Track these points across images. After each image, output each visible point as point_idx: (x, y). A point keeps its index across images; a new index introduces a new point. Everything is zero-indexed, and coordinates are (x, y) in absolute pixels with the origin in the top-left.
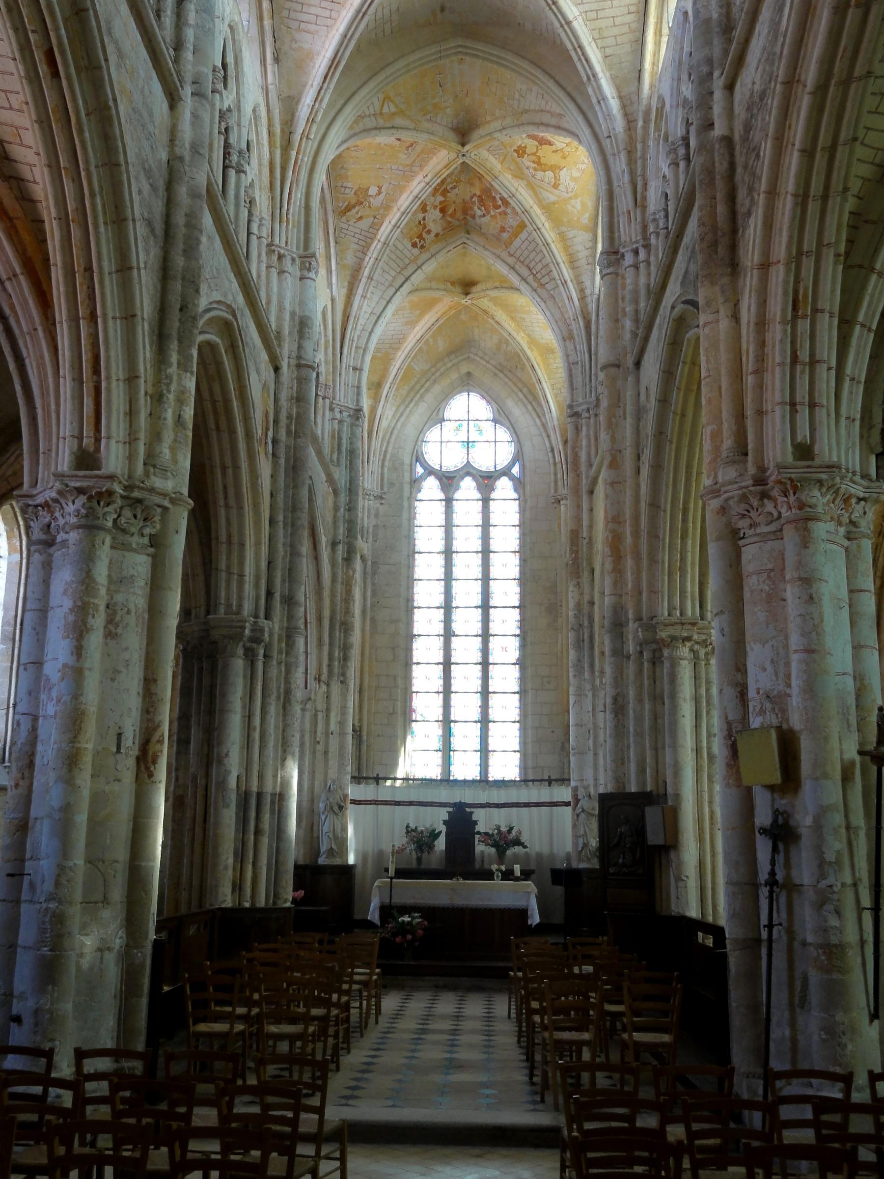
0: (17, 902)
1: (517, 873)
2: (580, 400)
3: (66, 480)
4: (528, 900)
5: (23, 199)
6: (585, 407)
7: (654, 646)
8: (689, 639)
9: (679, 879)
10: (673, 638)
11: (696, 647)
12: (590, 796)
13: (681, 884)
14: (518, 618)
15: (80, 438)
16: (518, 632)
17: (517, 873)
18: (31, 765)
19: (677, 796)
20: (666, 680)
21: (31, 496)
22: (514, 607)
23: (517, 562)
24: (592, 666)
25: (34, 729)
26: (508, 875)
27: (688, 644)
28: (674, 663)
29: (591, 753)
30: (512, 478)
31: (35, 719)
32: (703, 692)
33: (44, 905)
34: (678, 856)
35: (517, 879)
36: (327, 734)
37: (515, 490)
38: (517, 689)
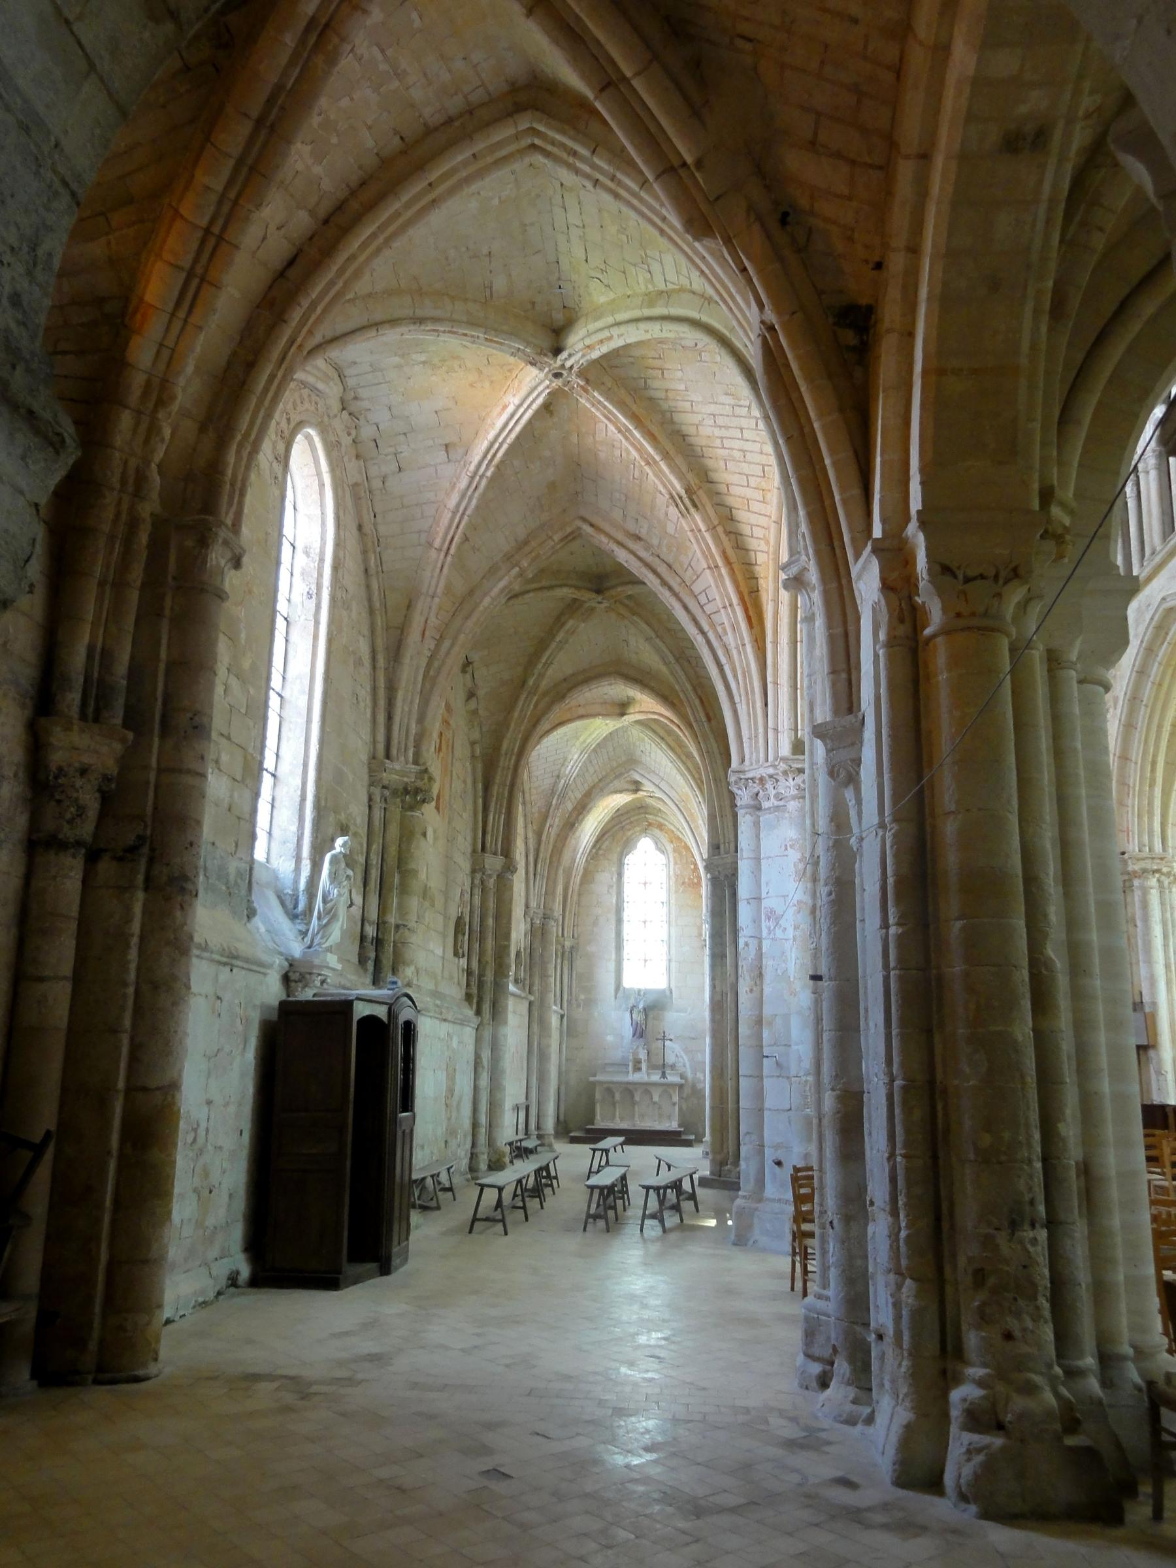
0: (761, 1078)
3: (790, 763)
5: (738, 547)
7: (1126, 877)
8: (1158, 871)
9: (1159, 1073)
10: (1144, 871)
11: (1163, 878)
13: (1161, 1078)
15: (796, 730)
18: (761, 975)
19: (1154, 1004)
20: (1137, 904)
21: (743, 772)
25: (760, 948)
27: (1157, 875)
28: (1145, 892)
31: (760, 941)
32: (1169, 915)
33: (804, 1078)
34: (1158, 1055)
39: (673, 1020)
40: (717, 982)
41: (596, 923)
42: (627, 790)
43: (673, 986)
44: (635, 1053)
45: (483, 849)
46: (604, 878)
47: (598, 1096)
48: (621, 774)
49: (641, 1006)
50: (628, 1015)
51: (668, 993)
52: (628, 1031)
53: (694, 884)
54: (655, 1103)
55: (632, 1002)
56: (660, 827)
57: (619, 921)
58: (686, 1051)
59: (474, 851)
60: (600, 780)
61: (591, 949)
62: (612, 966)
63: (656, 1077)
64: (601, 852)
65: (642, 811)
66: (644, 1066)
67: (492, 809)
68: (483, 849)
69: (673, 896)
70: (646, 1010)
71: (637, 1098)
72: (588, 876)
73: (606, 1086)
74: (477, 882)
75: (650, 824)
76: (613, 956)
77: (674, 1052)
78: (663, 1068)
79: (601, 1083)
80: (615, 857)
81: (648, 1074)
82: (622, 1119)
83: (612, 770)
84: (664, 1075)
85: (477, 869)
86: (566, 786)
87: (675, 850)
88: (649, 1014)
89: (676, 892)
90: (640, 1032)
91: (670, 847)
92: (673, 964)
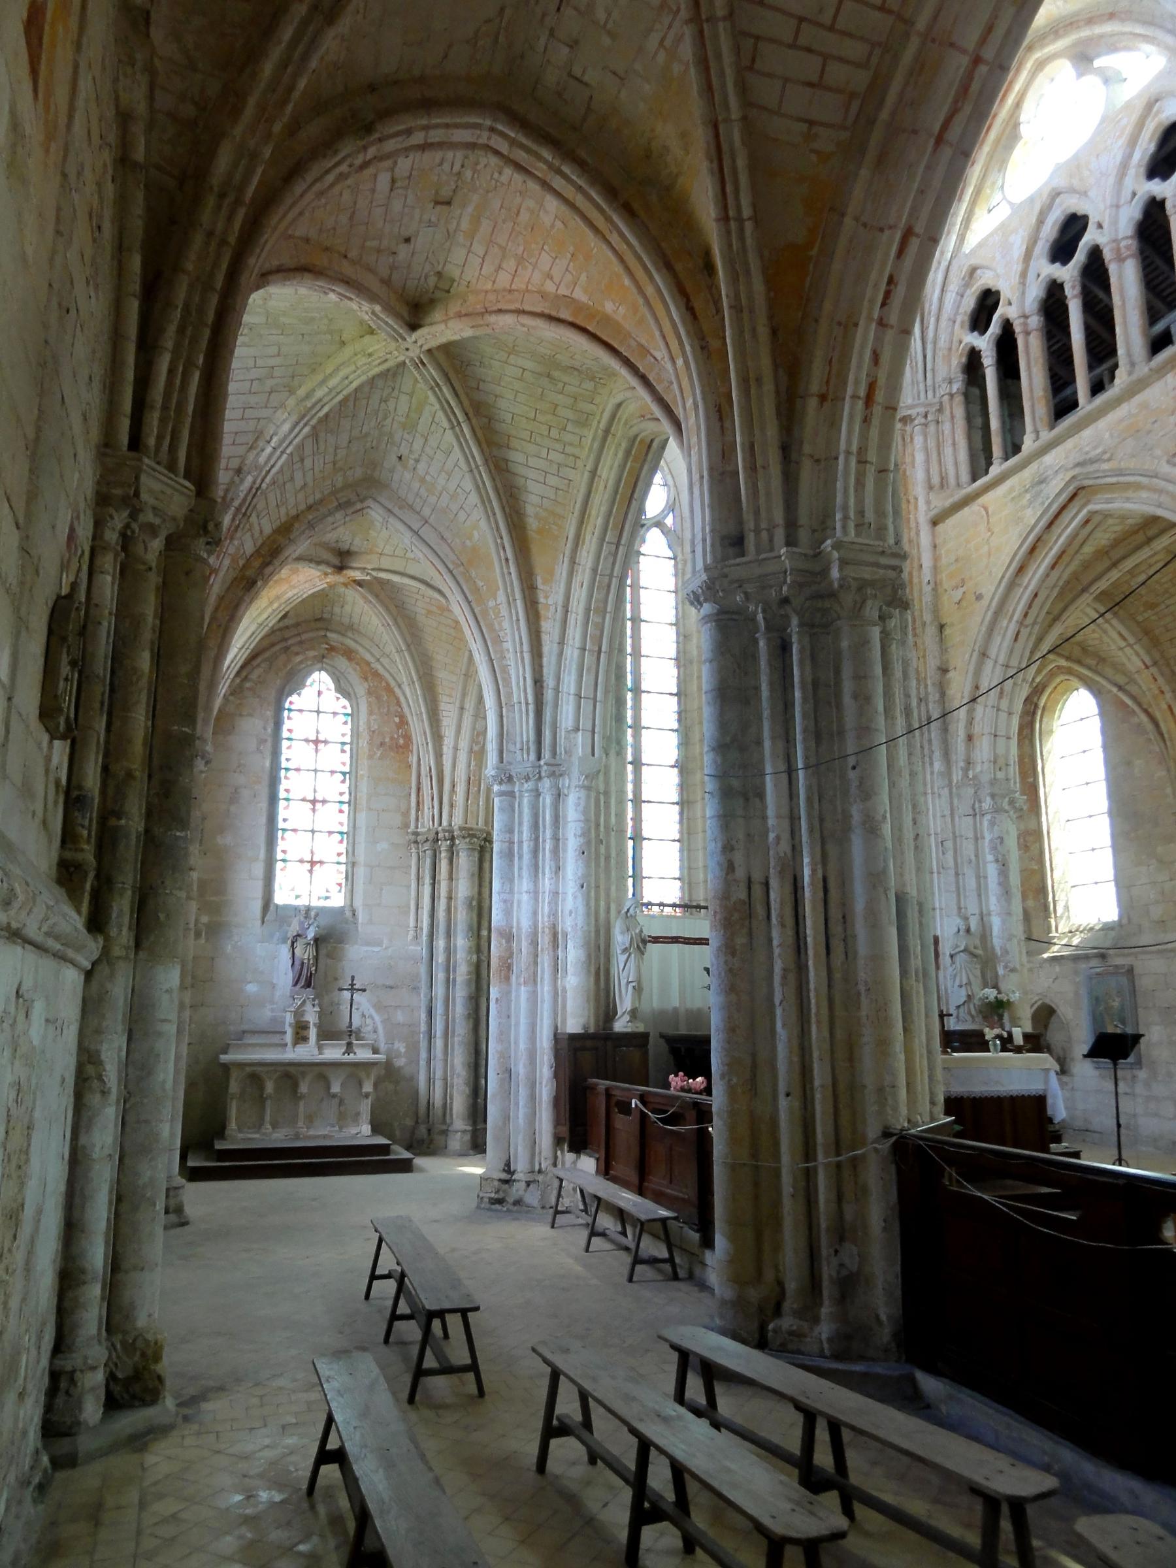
1: (1019, 1040)
2: (910, 401)
4: (1047, 1081)
6: (921, 410)
12: (968, 931)
14: (676, 708)
16: (675, 726)
17: (1019, 1040)
22: (671, 694)
23: (674, 637)
24: (946, 755)
26: (1007, 1043)
29: (952, 872)
30: (665, 531)
35: (1018, 1050)
36: (607, 827)
37: (670, 547)
38: (676, 798)
39: (360, 958)
40: (738, 858)
41: (234, 799)
42: (328, 564)
43: (358, 903)
44: (298, 1013)
45: (136, 443)
46: (251, 727)
47: (234, 1087)
48: (349, 503)
49: (311, 934)
50: (284, 952)
51: (348, 914)
52: (284, 975)
53: (398, 747)
54: (334, 1096)
55: (294, 928)
56: (349, 654)
57: (273, 799)
58: (379, 1007)
59: (107, 444)
60: (310, 508)
61: (227, 840)
62: (259, 869)
63: (334, 1053)
64: (248, 685)
65: (319, 625)
66: (313, 1033)
67: (169, 340)
68: (136, 443)
69: (364, 762)
70: (316, 940)
71: (304, 1088)
72: (225, 723)
73: (248, 1069)
74: (112, 536)
75: (332, 649)
76: (262, 854)
77: (363, 1010)
78: (350, 1036)
79: (241, 1065)
80: (272, 695)
81: (320, 1048)
82: (275, 1126)
83: (333, 493)
84: (349, 1048)
85: (113, 495)
86: (255, 491)
87: (369, 693)
88: (322, 948)
89: (371, 757)
90: (308, 978)
91: (361, 689)
92: (360, 871)
